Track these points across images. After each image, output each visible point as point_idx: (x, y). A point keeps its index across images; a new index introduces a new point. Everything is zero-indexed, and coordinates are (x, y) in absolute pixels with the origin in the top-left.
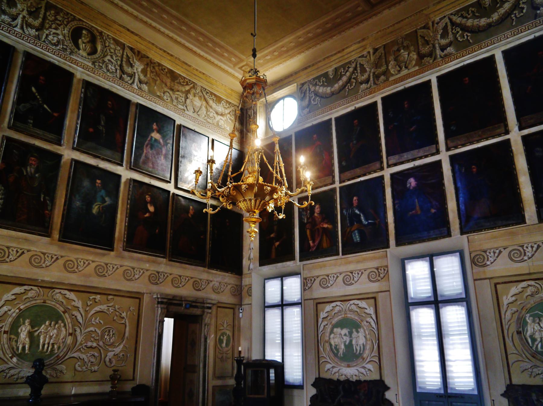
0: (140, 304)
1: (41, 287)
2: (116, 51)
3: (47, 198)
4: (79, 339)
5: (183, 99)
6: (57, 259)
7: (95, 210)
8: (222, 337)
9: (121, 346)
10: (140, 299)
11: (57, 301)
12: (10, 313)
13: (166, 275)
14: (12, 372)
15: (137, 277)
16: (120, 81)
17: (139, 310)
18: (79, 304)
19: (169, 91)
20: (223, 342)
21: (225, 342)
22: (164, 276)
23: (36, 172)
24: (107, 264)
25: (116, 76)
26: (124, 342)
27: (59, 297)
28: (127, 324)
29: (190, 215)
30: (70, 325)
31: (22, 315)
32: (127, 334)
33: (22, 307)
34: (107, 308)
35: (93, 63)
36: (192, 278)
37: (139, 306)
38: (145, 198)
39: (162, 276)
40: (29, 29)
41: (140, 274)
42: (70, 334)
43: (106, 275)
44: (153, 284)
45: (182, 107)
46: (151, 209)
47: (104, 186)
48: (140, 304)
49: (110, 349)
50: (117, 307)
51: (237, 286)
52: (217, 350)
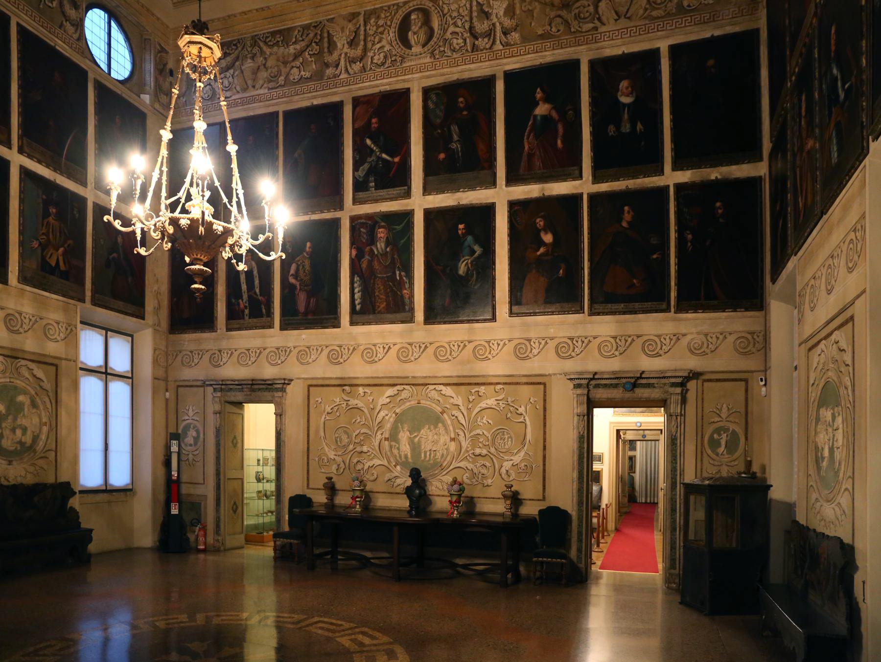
0: (545, 392)
1: (413, 385)
2: (461, 10)
3: (403, 274)
4: (465, 445)
5: (591, 9)
6: (426, 347)
7: (462, 269)
8: (715, 436)
9: (522, 454)
10: (545, 384)
11: (432, 399)
12: (387, 418)
13: (586, 341)
14: (398, 481)
15: (535, 351)
16: (474, 55)
17: (545, 400)
18: (459, 401)
19: (559, 12)
20: (719, 445)
21: (723, 443)
22: (583, 342)
23: (386, 247)
24: (488, 342)
25: (467, 50)
26: (525, 448)
27: (435, 395)
28: (528, 422)
29: (625, 224)
30: (451, 428)
31: (400, 419)
32: (529, 437)
33: (397, 411)
34: (496, 403)
35: (432, 54)
36: (638, 337)
37: (545, 396)
38: (535, 223)
39: (580, 343)
40: (353, 65)
41: (541, 346)
42: (453, 440)
43: (490, 356)
44: (563, 358)
45: (591, 25)
46: (548, 238)
47: (469, 231)
48: (545, 392)
49: (506, 458)
50: (509, 400)
51: (752, 333)
52: (706, 459)
